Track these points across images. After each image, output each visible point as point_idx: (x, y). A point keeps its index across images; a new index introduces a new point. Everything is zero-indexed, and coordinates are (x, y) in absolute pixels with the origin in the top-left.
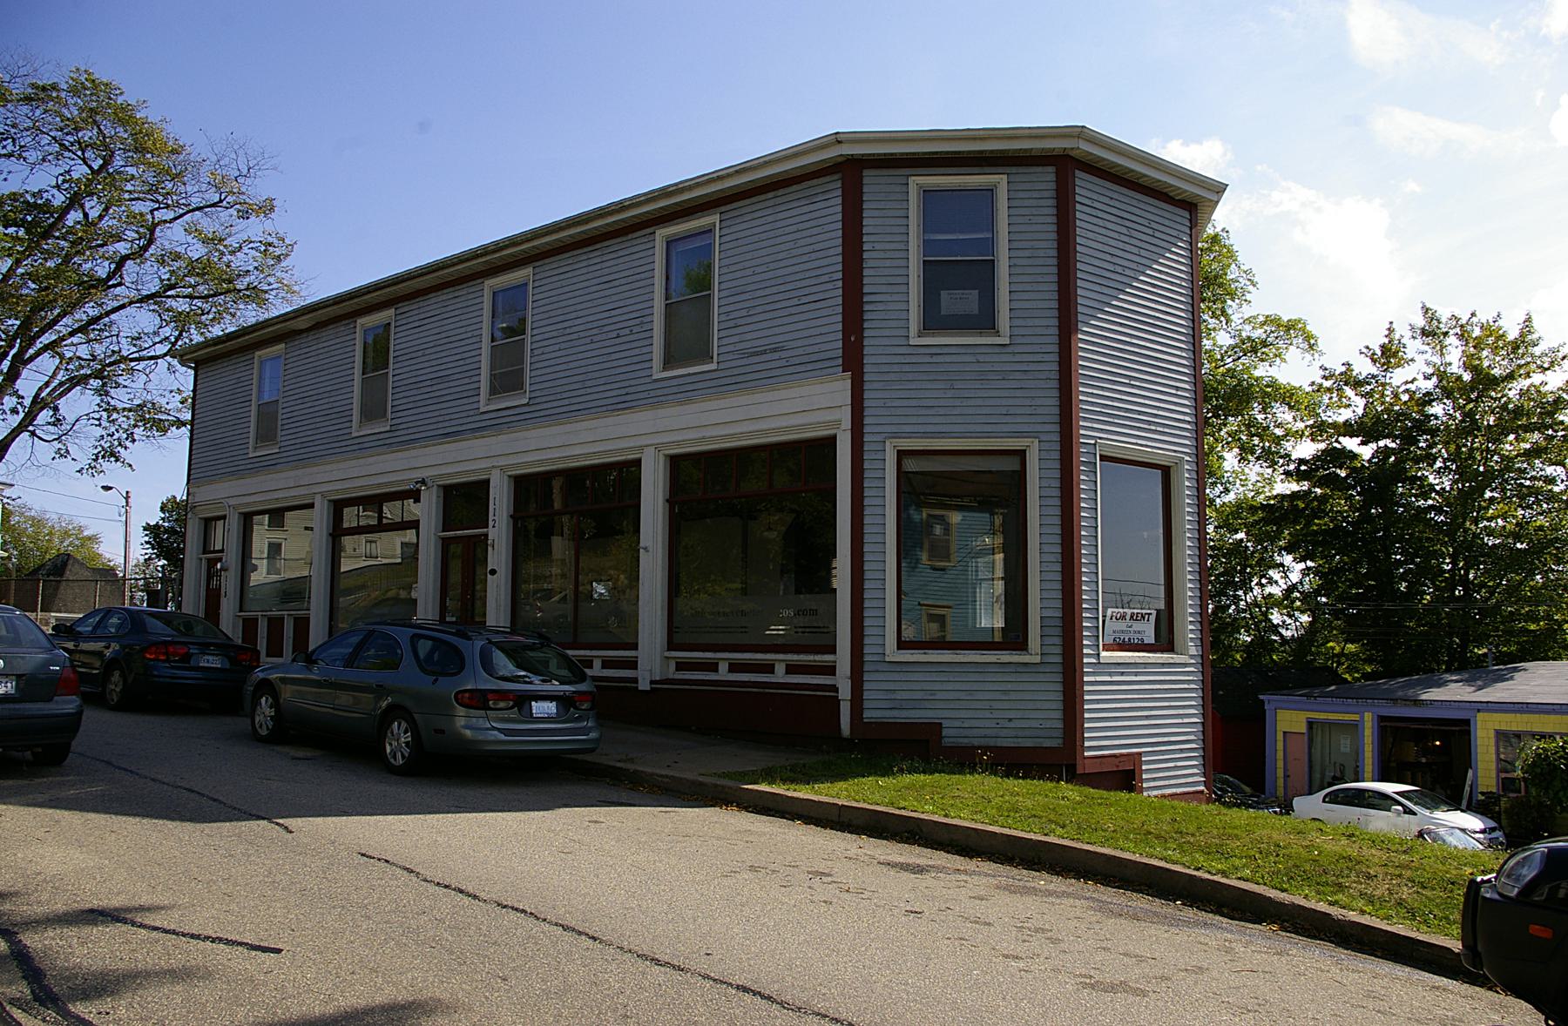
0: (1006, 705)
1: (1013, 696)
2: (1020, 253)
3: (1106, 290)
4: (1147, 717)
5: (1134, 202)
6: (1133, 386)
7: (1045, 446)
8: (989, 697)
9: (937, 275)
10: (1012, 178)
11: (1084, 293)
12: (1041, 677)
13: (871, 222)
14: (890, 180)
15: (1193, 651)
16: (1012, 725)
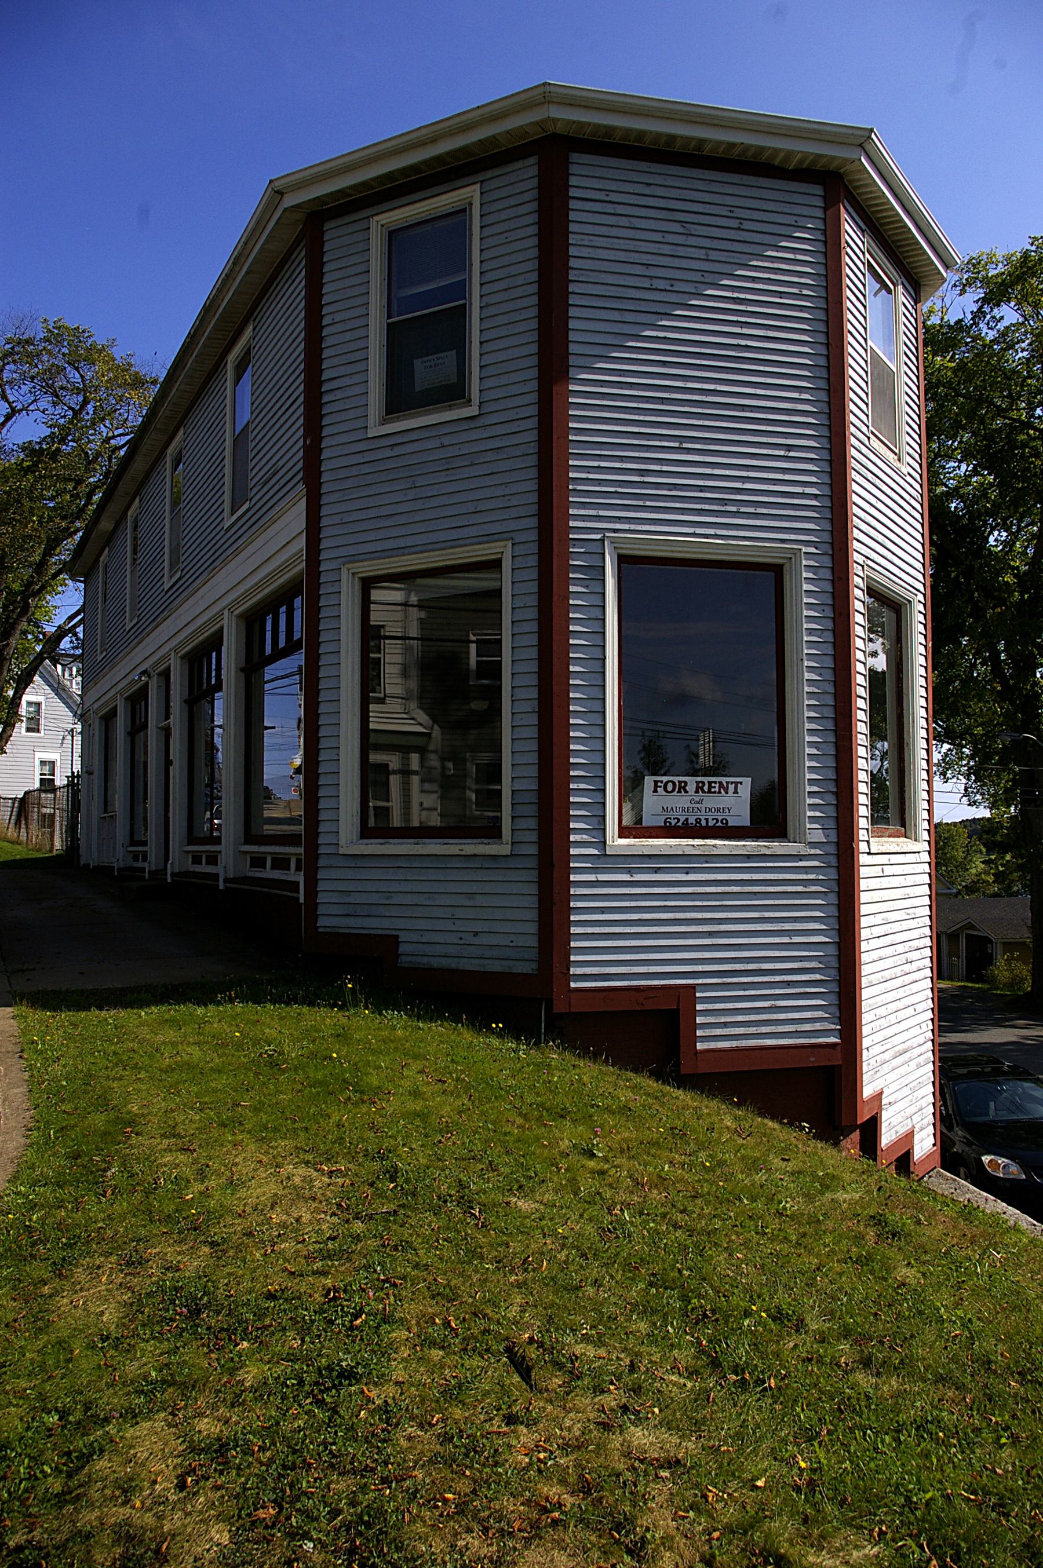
0: (470, 913)
1: (480, 901)
2: (494, 287)
3: (630, 317)
4: (711, 934)
5: (701, 185)
6: (689, 451)
7: (520, 550)
8: (450, 904)
9: (405, 342)
10: (487, 186)
11: (581, 327)
12: (513, 876)
13: (329, 290)
14: (350, 229)
15: (819, 836)
16: (476, 941)
